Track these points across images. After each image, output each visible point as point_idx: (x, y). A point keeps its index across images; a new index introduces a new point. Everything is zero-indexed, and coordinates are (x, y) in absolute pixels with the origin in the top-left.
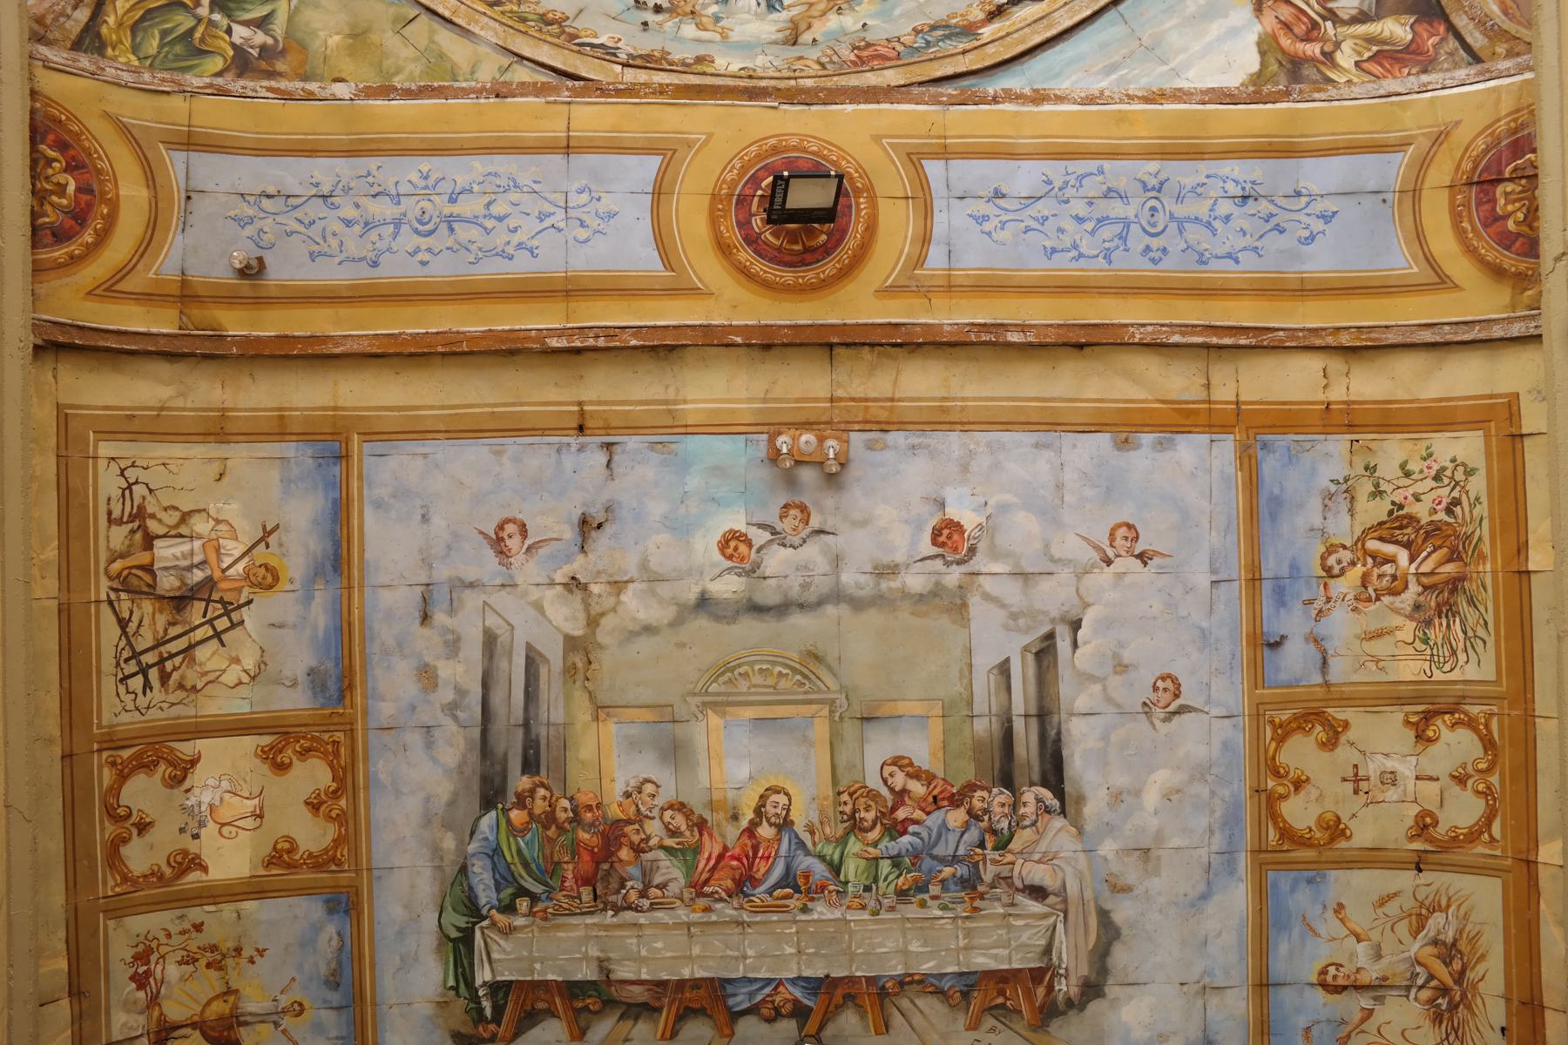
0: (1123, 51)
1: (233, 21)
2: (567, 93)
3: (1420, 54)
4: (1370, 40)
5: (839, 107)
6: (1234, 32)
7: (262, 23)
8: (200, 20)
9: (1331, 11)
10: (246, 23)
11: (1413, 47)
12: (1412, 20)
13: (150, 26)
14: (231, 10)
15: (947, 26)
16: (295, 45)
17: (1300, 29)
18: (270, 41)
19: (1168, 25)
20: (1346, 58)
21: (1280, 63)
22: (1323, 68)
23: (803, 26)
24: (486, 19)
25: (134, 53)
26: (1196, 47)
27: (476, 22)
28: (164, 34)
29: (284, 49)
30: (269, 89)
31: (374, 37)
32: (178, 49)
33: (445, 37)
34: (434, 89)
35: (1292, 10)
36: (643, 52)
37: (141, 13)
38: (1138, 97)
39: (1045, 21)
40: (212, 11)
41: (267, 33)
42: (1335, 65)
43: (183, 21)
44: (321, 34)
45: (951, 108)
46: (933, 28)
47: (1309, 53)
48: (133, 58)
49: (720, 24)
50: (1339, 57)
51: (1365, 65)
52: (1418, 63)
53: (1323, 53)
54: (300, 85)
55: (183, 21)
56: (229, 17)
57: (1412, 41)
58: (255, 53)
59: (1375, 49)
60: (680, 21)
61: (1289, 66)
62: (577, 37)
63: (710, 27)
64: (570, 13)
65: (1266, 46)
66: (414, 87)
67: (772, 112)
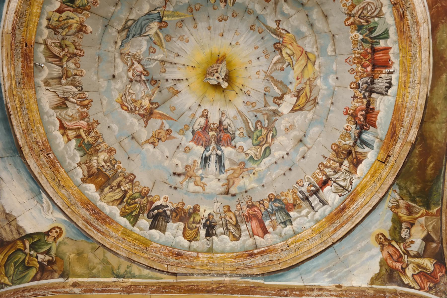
0: (334, 263)
1: (38, 253)
2: (149, 292)
3: (435, 278)
4: (419, 266)
5: (236, 295)
6: (372, 257)
7: (48, 253)
8: (26, 254)
9: (407, 251)
10: (42, 253)
11: (433, 274)
12: (434, 262)
13: (11, 262)
14: (37, 249)
15: (280, 200)
16: (59, 258)
17: (395, 257)
18: (51, 258)
19: (350, 253)
20: (409, 272)
21: (386, 270)
22: (401, 274)
23: (231, 183)
24: (122, 249)
25: (6, 276)
26: (358, 263)
27: (119, 249)
28: (15, 263)
29: (55, 260)
30: (53, 292)
31: (85, 255)
32: (20, 268)
33: (109, 256)
34: (106, 290)
35: (394, 249)
36: (175, 207)
37: (7, 258)
38: (334, 295)
39: (308, 252)
40: (30, 251)
41: (49, 255)
42: (405, 274)
43: (21, 256)
44: (68, 254)
45: (272, 297)
46: (276, 200)
47: (397, 267)
48: (6, 278)
49: (202, 182)
50: (407, 270)
51: (415, 277)
52: (433, 282)
53: (402, 268)
54: (63, 289)
55: (21, 256)
56: (36, 252)
57: (433, 271)
58: (46, 263)
59: (420, 270)
60: (189, 181)
61: (389, 272)
62: (153, 203)
63: (199, 184)
64: (150, 188)
65: (383, 263)
66: (100, 290)
67: (215, 296)
